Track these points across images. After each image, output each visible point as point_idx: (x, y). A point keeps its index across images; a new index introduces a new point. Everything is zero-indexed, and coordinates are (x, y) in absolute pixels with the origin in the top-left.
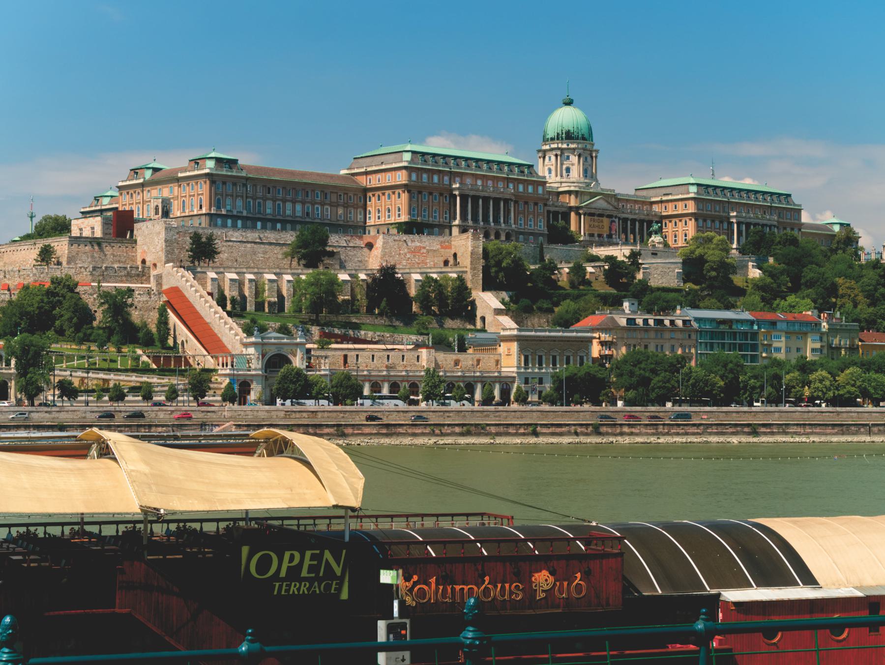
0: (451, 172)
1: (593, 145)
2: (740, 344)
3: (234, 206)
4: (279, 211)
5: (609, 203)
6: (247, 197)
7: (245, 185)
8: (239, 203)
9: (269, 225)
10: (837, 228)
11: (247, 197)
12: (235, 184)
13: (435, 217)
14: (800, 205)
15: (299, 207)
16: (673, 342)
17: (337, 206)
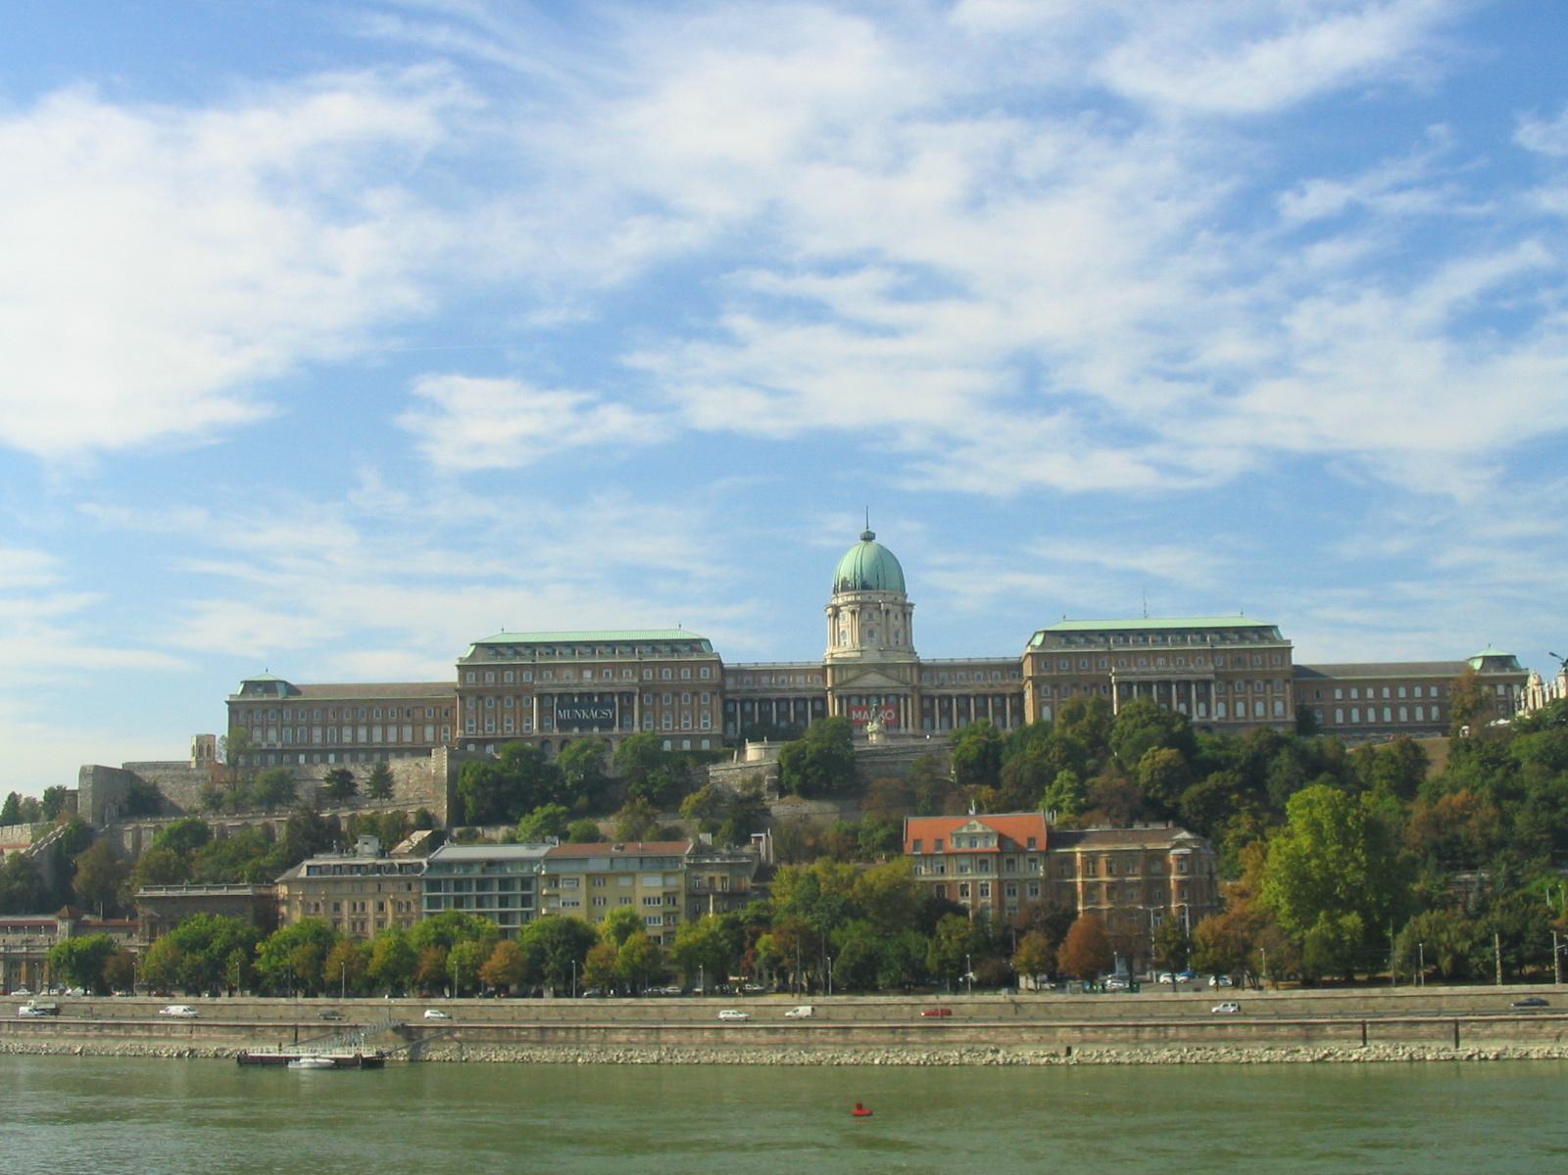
0: (534, 666)
1: (906, 597)
2: (456, 898)
3: (265, 736)
4: (332, 739)
5: (889, 677)
6: (282, 726)
7: (280, 711)
8: (272, 734)
9: (362, 756)
10: (1477, 665)
11: (282, 726)
12: (265, 711)
13: (509, 728)
14: (1289, 642)
15: (408, 731)
16: (380, 898)
17: (424, 723)
